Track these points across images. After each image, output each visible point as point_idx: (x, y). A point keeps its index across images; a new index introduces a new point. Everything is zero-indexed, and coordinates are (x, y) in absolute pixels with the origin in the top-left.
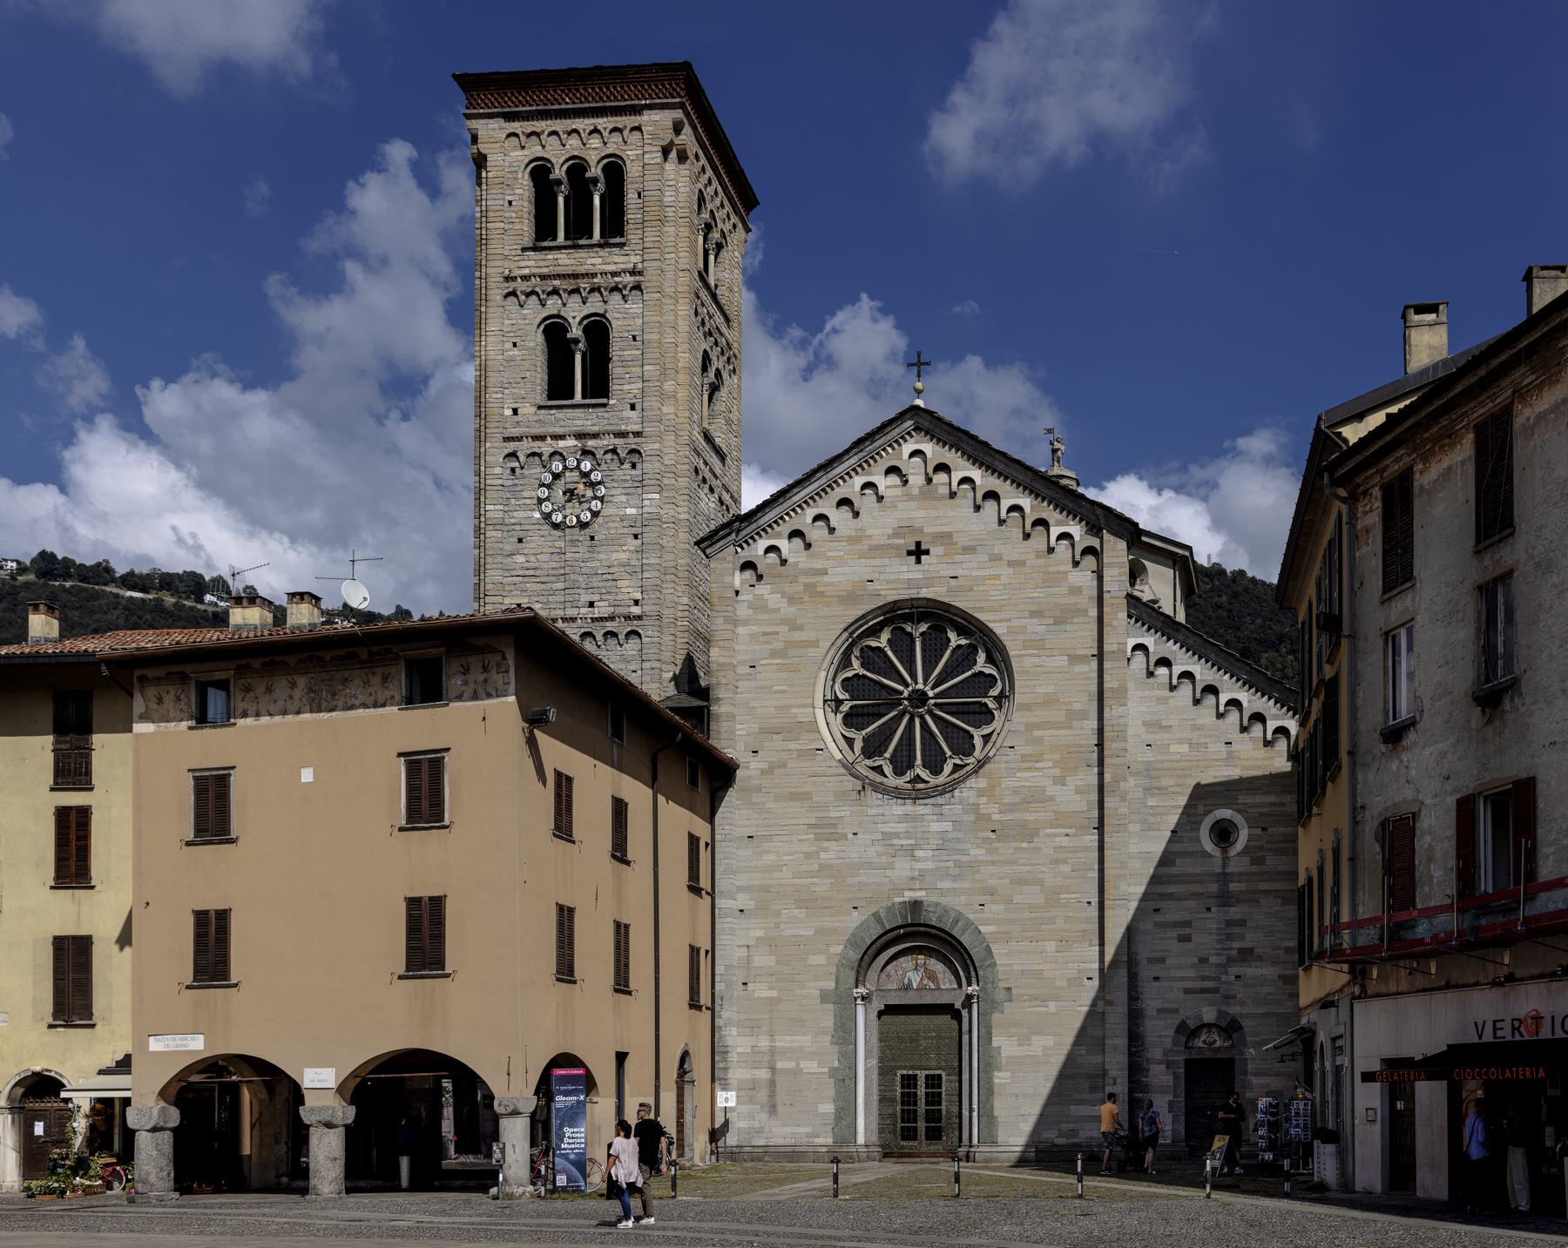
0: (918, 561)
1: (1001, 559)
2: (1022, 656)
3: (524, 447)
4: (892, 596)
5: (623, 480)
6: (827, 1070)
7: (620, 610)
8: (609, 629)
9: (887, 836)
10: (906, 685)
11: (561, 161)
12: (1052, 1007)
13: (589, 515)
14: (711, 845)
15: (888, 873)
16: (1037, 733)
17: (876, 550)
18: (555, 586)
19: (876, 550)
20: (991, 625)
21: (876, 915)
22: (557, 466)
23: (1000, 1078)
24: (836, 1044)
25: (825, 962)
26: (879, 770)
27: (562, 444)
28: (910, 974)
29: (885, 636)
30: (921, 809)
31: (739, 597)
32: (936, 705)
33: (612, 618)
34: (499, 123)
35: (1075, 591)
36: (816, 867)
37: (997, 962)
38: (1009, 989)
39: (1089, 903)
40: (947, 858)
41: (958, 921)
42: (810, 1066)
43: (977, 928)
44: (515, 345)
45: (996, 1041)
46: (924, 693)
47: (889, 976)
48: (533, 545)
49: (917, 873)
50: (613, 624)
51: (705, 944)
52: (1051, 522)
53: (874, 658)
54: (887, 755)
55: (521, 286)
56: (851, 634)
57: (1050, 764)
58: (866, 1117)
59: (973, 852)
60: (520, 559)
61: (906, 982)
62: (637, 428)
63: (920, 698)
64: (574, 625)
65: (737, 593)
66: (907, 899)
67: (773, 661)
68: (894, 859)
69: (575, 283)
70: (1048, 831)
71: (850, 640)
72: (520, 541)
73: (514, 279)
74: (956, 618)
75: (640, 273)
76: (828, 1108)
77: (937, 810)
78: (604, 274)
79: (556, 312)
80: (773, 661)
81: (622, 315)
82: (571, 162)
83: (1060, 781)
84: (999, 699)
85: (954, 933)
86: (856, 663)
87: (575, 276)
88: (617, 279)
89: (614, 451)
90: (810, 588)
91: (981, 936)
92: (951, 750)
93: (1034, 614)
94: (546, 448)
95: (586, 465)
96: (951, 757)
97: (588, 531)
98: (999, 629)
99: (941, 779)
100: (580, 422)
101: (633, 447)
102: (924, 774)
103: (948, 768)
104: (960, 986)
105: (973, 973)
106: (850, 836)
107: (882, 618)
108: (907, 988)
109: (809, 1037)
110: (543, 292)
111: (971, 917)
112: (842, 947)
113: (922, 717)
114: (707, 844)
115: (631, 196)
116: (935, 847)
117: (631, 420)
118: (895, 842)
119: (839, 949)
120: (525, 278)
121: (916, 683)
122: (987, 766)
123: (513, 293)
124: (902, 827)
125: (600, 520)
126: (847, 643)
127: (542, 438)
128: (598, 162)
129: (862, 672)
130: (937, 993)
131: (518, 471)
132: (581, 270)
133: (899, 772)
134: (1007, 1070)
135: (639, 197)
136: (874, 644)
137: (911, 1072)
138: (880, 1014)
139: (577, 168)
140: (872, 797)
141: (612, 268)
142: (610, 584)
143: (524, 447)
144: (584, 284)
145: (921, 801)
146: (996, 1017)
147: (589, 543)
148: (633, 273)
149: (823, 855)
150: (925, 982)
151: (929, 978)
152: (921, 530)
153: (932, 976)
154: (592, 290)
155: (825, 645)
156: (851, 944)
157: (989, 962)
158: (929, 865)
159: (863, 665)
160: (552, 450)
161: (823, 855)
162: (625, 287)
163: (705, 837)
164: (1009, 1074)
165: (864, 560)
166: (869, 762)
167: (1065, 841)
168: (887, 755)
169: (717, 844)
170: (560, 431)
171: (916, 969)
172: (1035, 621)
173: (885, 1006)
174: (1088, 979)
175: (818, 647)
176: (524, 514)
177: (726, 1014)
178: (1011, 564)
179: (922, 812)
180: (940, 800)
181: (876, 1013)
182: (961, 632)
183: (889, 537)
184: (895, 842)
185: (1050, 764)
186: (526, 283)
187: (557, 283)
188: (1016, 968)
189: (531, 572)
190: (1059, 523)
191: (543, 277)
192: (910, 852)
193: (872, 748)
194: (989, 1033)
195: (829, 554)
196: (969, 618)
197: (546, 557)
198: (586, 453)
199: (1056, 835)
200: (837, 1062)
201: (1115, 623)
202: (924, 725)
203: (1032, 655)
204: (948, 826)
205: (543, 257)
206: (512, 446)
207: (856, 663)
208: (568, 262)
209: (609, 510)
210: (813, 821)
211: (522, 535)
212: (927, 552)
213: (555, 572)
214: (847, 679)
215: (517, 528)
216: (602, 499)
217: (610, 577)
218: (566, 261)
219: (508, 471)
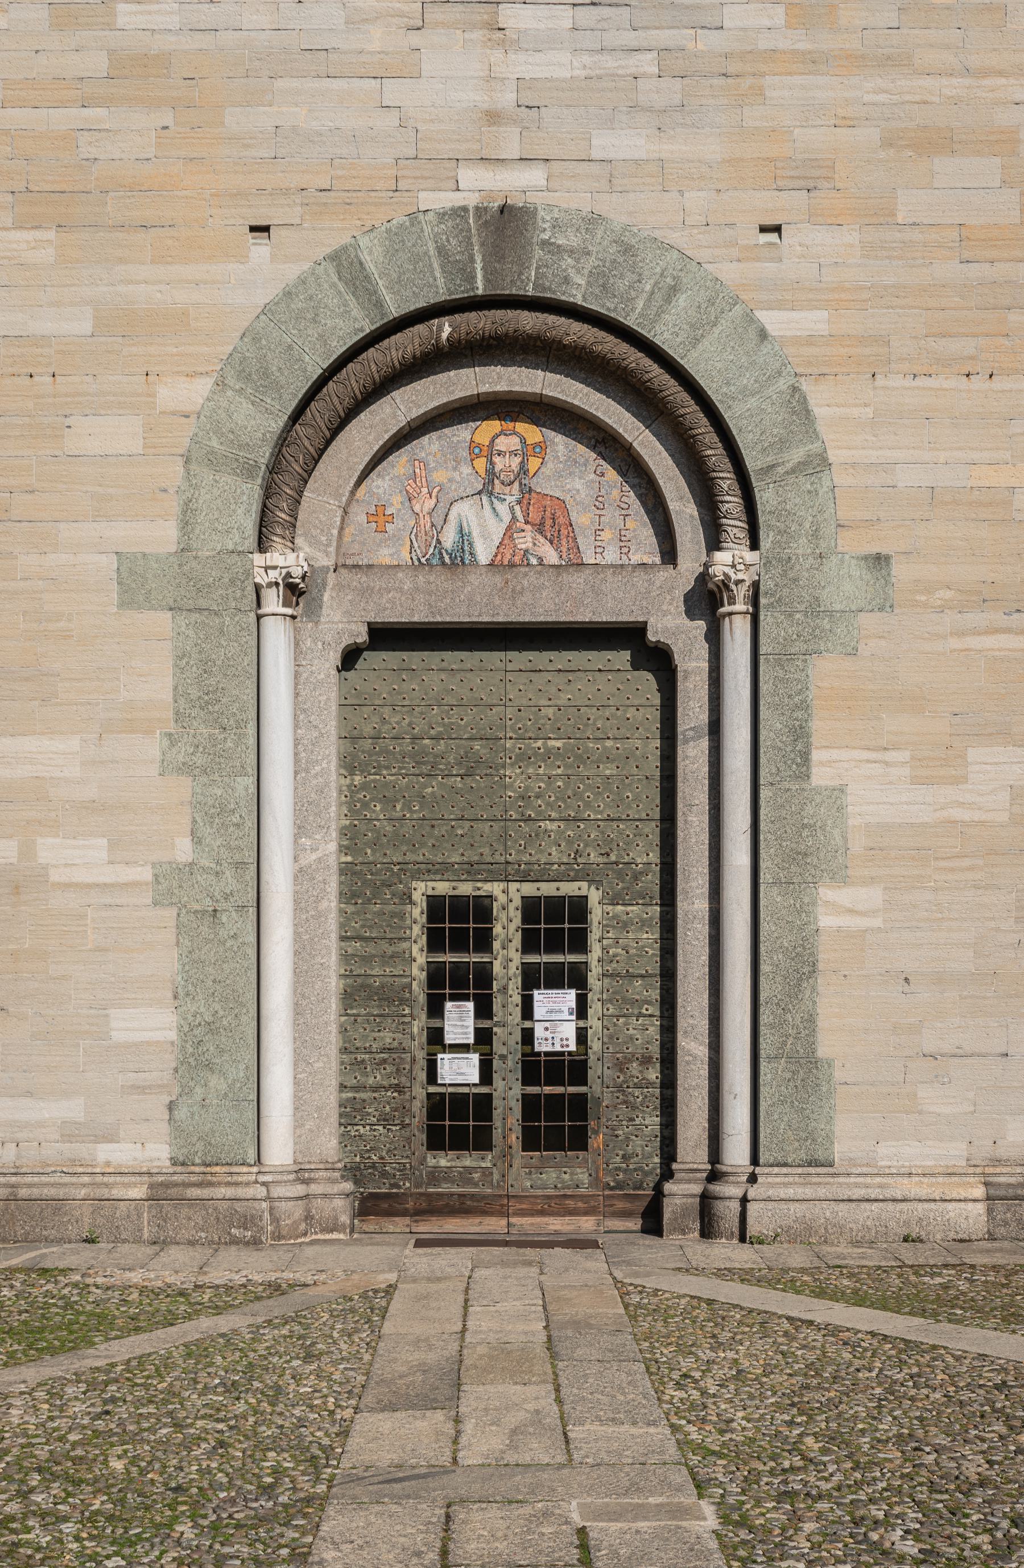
6: (146, 874)
15: (394, 91)
24: (186, 769)
25: (136, 446)
28: (464, 510)
36: (97, 63)
37: (833, 456)
38: (879, 561)
40: (630, 38)
41: (674, 290)
43: (750, 318)
47: (380, 516)
49: (507, 98)
58: (299, 1060)
61: (449, 538)
66: (471, 200)
68: (415, 39)
85: (662, 337)
91: (766, 348)
104: (669, 554)
105: (731, 503)
109: (74, 743)
111: (729, 272)
112: (204, 386)
130: (577, 580)
134: (872, 880)
137: (466, 889)
150: (525, 540)
151: (540, 528)
156: (244, 376)
157: (796, 455)
164: (870, 896)
171: (487, 490)
181: (335, 658)
188: (907, 478)
194: (800, 734)
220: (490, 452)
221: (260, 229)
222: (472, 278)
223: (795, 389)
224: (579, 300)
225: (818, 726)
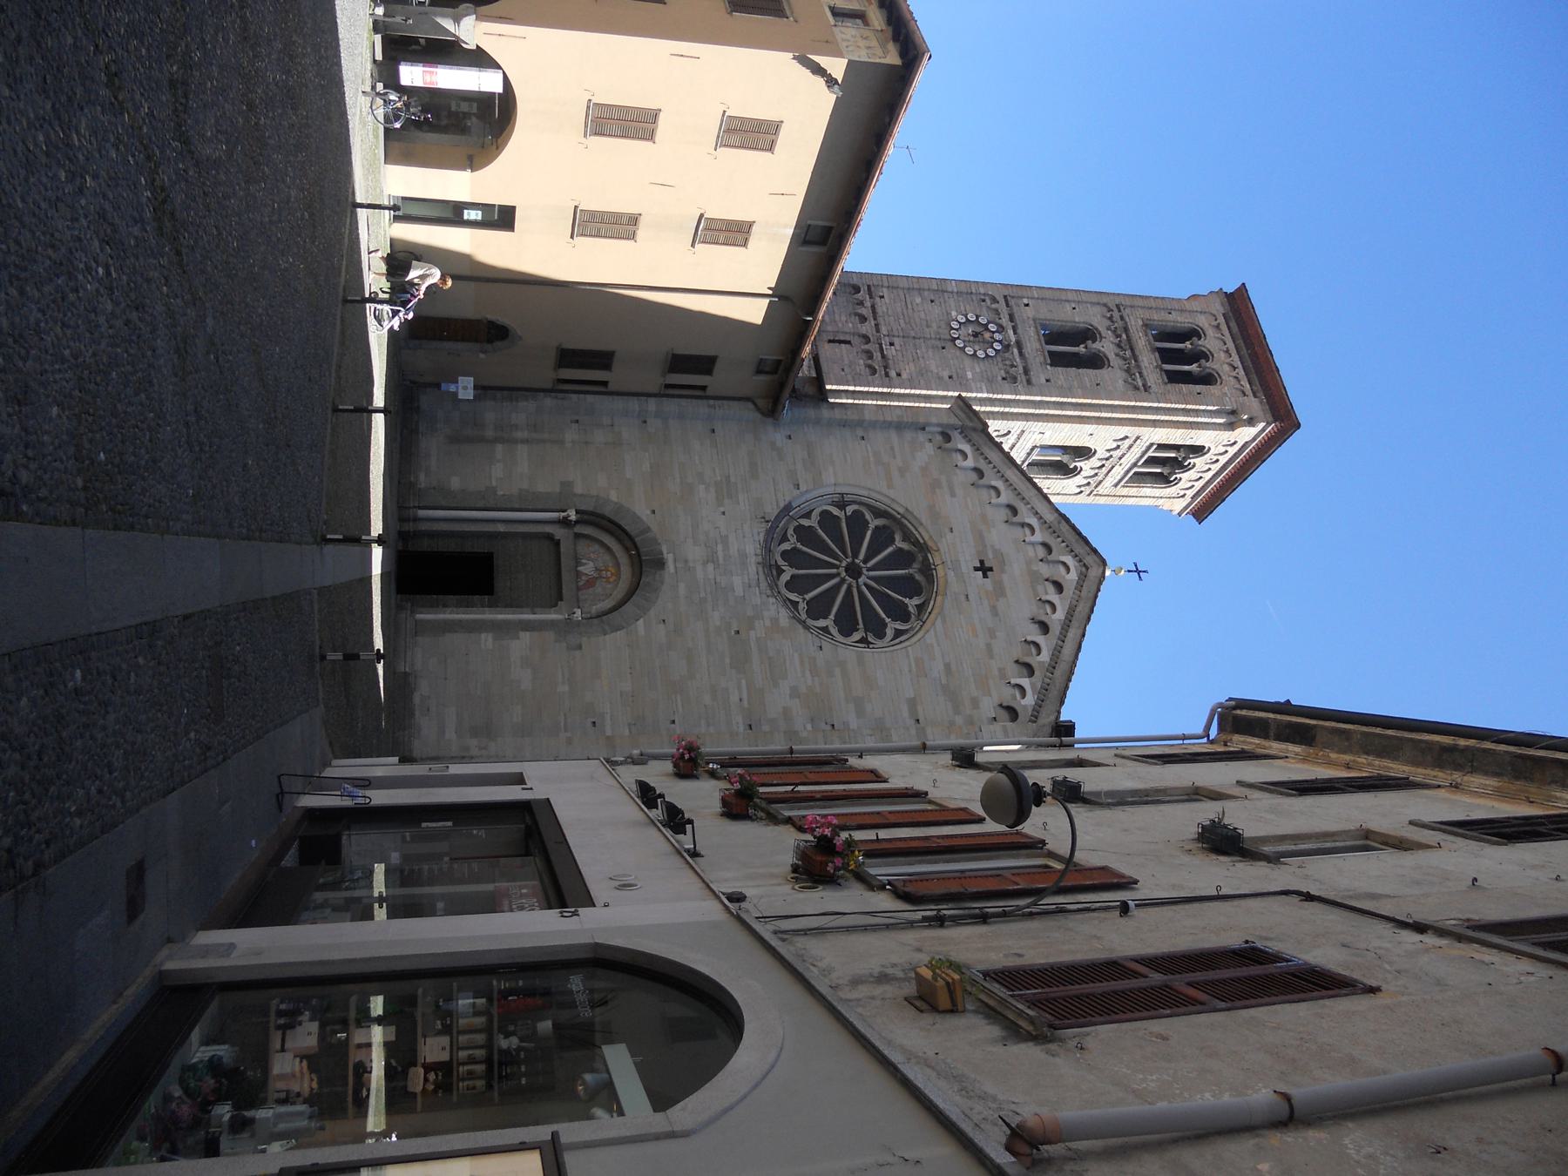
0: (976, 569)
1: (992, 638)
2: (908, 656)
4: (943, 547)
5: (992, 372)
6: (494, 484)
7: (891, 362)
8: (875, 354)
9: (725, 540)
10: (865, 561)
11: (1208, 346)
12: (566, 688)
13: (962, 345)
14: (700, 392)
16: (837, 671)
17: (980, 537)
18: (902, 321)
19: (980, 537)
20: (932, 632)
21: (648, 529)
22: (992, 327)
23: (487, 640)
26: (784, 539)
27: (1011, 332)
29: (905, 546)
30: (752, 569)
31: (920, 433)
32: (850, 587)
33: (883, 356)
34: (1222, 310)
35: (975, 703)
37: (607, 636)
38: (580, 647)
39: (673, 722)
42: (497, 471)
43: (641, 617)
44: (1074, 308)
45: (526, 637)
46: (860, 574)
48: (930, 309)
49: (691, 565)
50: (880, 358)
51: (616, 377)
52: (1033, 679)
53: (882, 538)
54: (799, 546)
55: (1116, 315)
56: (903, 516)
57: (810, 682)
59: (716, 614)
60: (918, 300)
61: (584, 561)
62: (1034, 380)
63: (854, 571)
64: (874, 332)
65: (924, 429)
66: (665, 556)
67: (871, 454)
69: (1126, 344)
70: (744, 682)
71: (899, 516)
72: (932, 301)
73: (1120, 311)
74: (932, 603)
75: (1146, 391)
76: (455, 483)
77: (754, 583)
78: (1138, 366)
79: (1104, 335)
80: (871, 454)
81: (1114, 375)
82: (1208, 353)
83: (795, 693)
84: (863, 641)
86: (879, 522)
87: (1132, 350)
88: (1137, 374)
89: (1012, 366)
90: (935, 485)
92: (812, 599)
93: (947, 666)
94: (1005, 321)
95: (997, 346)
96: (804, 599)
97: (949, 345)
98: (930, 638)
99: (784, 591)
100: (1028, 345)
101: (1019, 378)
102: (785, 577)
103: (793, 597)
106: (722, 509)
107: (922, 541)
108: (577, 562)
110: (1116, 328)
111: (652, 613)
113: (838, 574)
114: (704, 388)
115: (1198, 388)
116: (718, 580)
117: (1039, 376)
118: (720, 547)
119: (614, 496)
120: (1122, 318)
121: (869, 570)
122: (800, 626)
123: (1110, 310)
124: (734, 550)
125: (958, 353)
126: (895, 513)
127: (1012, 318)
128: (1213, 369)
129: (872, 526)
131: (983, 303)
132: (1137, 353)
133: (784, 554)
135: (1199, 394)
136: (898, 537)
138: (550, 537)
140: (763, 527)
141: (1145, 373)
142: (911, 358)
143: (1002, 306)
144: (1128, 353)
145: (760, 569)
146: (550, 636)
147: (940, 346)
148: (1144, 385)
149: (702, 487)
152: (1003, 571)
153: (591, 583)
154: (1125, 359)
155: (891, 493)
157: (607, 628)
158: (700, 574)
159: (877, 527)
160: (1004, 325)
161: (702, 487)
162: (1134, 380)
163: (715, 382)
164: (491, 647)
165: (968, 525)
166: (790, 531)
167: (734, 698)
168: (799, 546)
169: (705, 401)
170: (1019, 331)
171: (597, 569)
172: (941, 667)
173: (559, 540)
174: (594, 723)
175: (889, 488)
176: (953, 304)
177: (549, 402)
178: (989, 646)
179: (750, 569)
180: (764, 585)
181: (551, 531)
182: (921, 608)
183: (992, 546)
184: (720, 547)
185: (810, 682)
186: (1119, 317)
187: (1124, 336)
189: (910, 306)
190: (1033, 685)
191: (1126, 330)
192: (711, 559)
193: (804, 534)
195: (968, 499)
196: (934, 612)
197: (923, 316)
198: (1007, 347)
199: (739, 688)
200: (502, 493)
201: (953, 736)
202: (832, 576)
203: (910, 665)
204: (739, 591)
205: (1139, 329)
206: (1002, 301)
207: (879, 522)
208: (1140, 345)
209: (968, 362)
210: (733, 479)
211: (937, 302)
212: (985, 576)
213: (912, 321)
214: (863, 515)
215: (942, 300)
216: (975, 355)
217: (915, 357)
218: (1142, 342)
219: (983, 297)
220: (607, 570)
221: (654, 512)
222: (646, 556)
223: (623, 628)
224: (643, 579)
225: (536, 634)
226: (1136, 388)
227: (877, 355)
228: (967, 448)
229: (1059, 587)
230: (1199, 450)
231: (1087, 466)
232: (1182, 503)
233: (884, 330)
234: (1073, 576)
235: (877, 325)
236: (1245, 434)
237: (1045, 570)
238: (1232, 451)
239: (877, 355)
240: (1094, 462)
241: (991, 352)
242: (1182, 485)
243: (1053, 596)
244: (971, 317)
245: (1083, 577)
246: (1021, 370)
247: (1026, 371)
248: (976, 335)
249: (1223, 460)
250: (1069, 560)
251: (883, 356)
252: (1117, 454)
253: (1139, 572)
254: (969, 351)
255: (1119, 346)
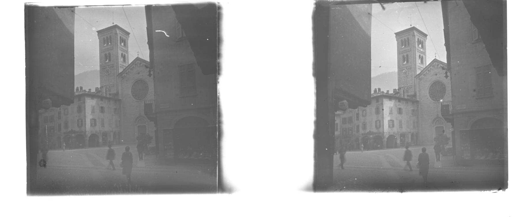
3: (401, 69)
94: (403, 69)
95: (407, 70)
139: (405, 39)
144: (406, 51)
198: (407, 69)
226: (411, 50)
227: (409, 87)
228: (421, 76)
229: (438, 65)
230: (418, 39)
231: (421, 55)
232: (425, 38)
233: (406, 86)
234: (437, 63)
235: (406, 87)
236: (416, 33)
237: (436, 67)
238: (418, 34)
239: (409, 87)
240: (421, 54)
241: (407, 71)
242: (423, 40)
243: (439, 66)
244: (403, 74)
245: (436, 62)
246: (409, 67)
247: (410, 66)
248: (405, 73)
249: (419, 35)
250: (434, 64)
251: (409, 86)
252: (419, 51)
253: (436, 54)
254: (407, 74)
255: (405, 52)
